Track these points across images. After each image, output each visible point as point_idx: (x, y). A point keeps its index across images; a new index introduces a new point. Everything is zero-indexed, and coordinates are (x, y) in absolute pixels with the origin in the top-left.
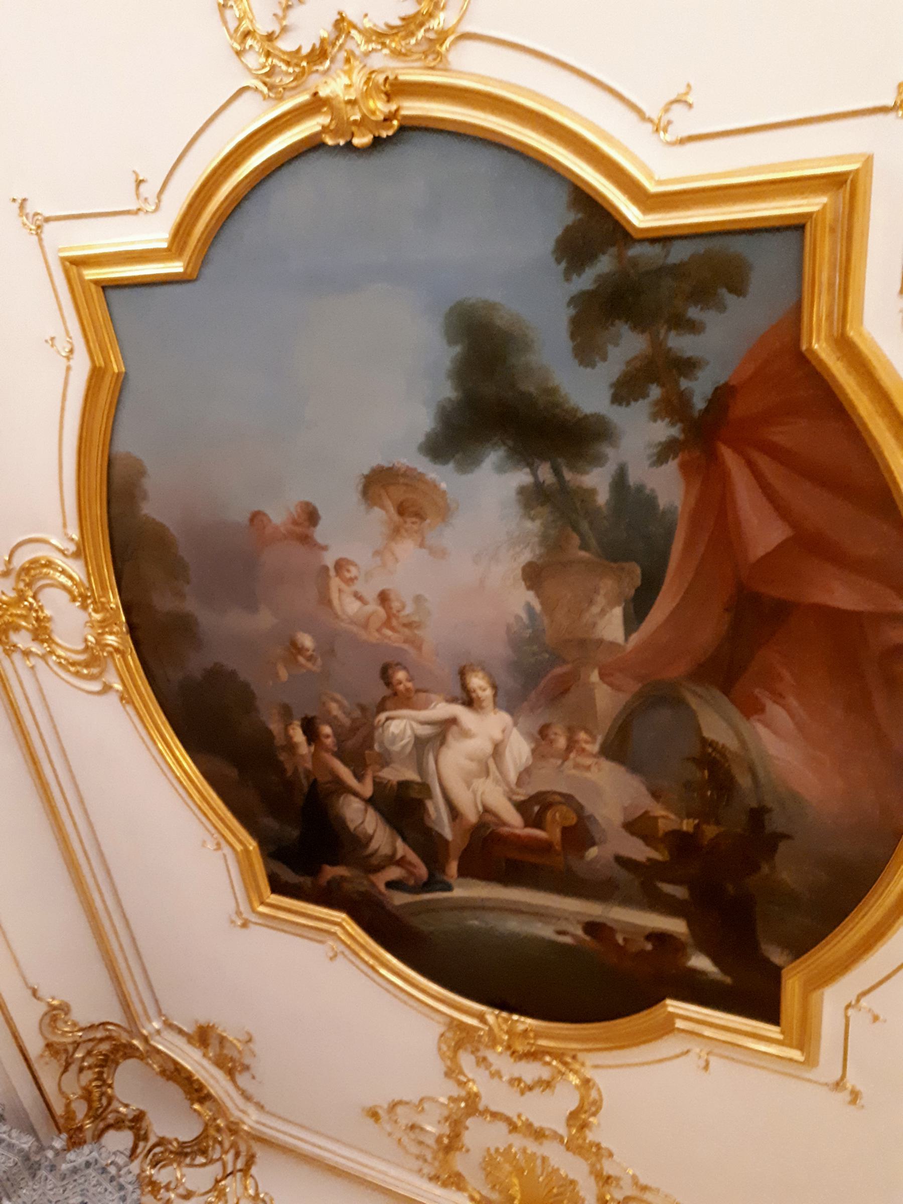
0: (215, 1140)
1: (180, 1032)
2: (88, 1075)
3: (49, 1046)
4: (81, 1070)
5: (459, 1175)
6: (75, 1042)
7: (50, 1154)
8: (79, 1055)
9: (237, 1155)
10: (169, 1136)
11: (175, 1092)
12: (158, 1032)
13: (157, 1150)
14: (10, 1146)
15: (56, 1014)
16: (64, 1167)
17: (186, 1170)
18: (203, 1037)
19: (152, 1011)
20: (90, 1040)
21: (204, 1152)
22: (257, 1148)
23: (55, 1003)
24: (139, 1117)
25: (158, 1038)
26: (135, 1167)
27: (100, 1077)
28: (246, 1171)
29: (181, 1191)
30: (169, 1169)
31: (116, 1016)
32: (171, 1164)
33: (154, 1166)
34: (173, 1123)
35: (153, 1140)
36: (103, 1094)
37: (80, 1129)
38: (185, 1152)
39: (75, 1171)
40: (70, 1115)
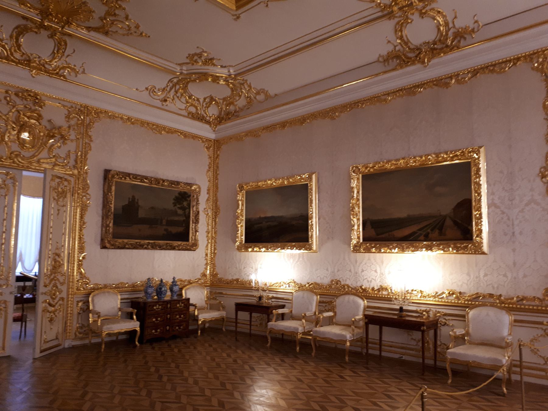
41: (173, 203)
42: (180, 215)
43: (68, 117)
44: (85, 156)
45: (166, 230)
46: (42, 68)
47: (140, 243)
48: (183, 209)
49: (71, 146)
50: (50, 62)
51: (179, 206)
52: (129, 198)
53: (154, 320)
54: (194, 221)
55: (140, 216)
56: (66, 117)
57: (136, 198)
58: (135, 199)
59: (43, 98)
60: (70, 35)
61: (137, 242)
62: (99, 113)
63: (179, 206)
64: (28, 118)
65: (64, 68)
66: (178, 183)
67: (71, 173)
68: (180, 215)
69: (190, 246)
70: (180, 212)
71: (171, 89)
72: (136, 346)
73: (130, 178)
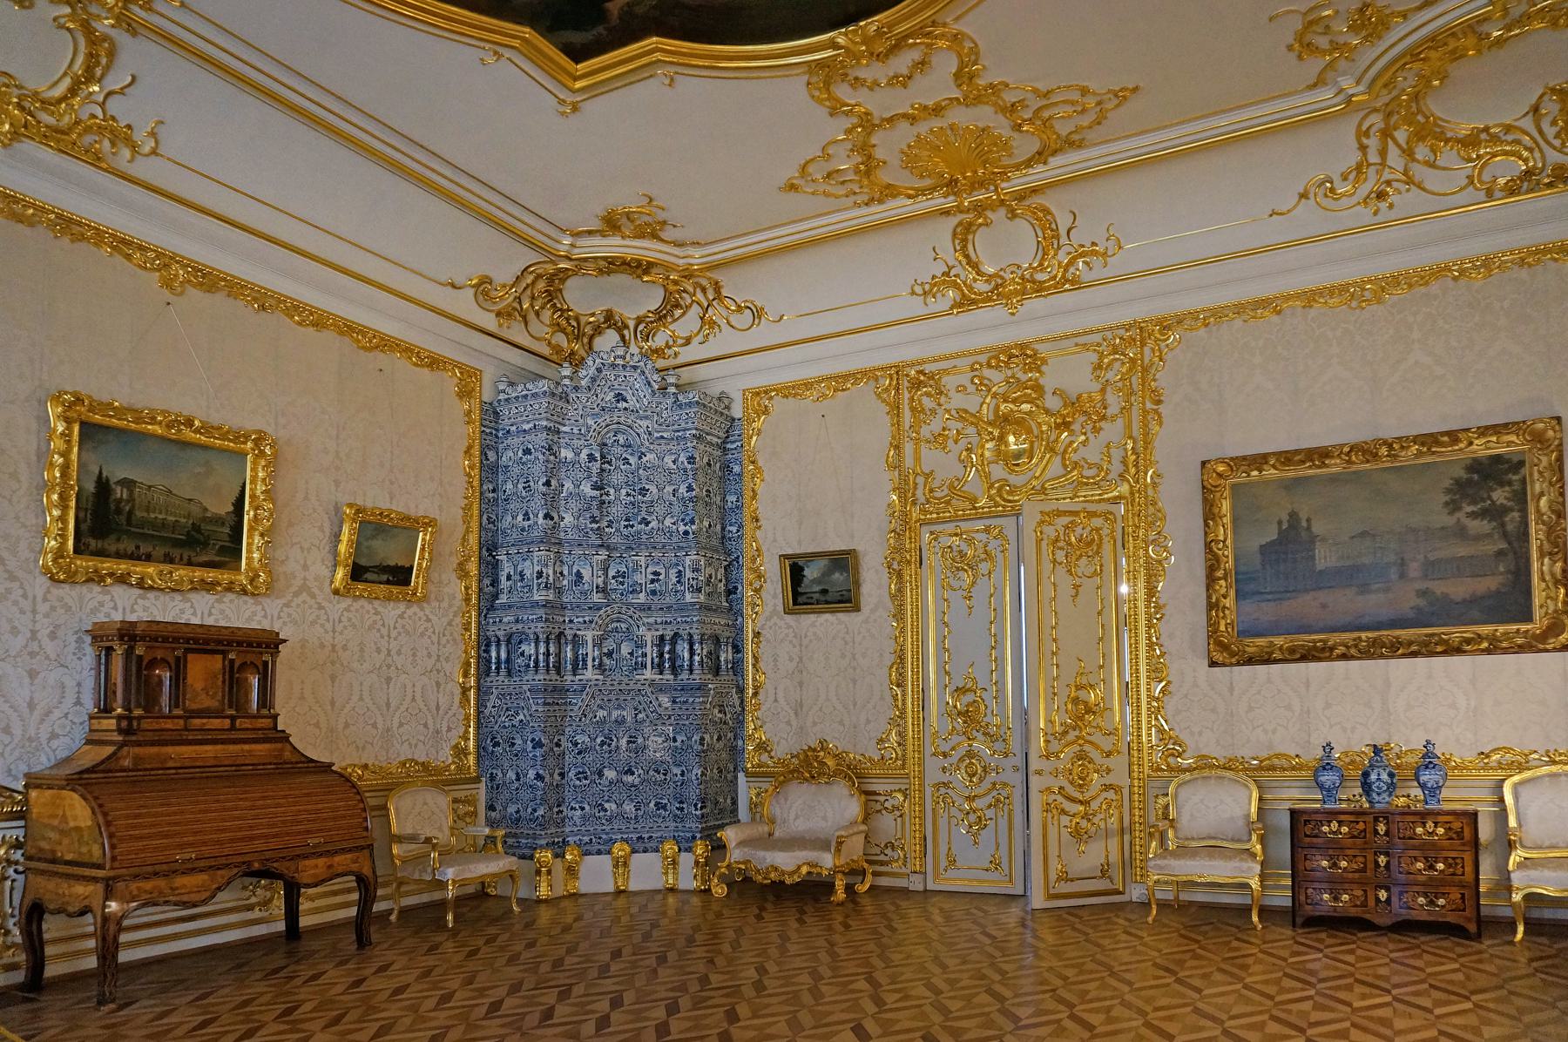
0: (679, 292)
1: (590, 233)
2: (547, 314)
3: (499, 314)
4: (537, 314)
5: (889, 186)
7: (567, 382)
9: (704, 290)
10: (642, 312)
12: (572, 245)
13: (641, 327)
15: (483, 288)
16: (583, 383)
18: (611, 224)
21: (677, 306)
22: (715, 275)
24: (609, 316)
26: (634, 349)
27: (555, 309)
29: (680, 341)
34: (641, 300)
35: (632, 324)
36: (568, 319)
37: (572, 353)
38: (661, 316)
39: (593, 380)
40: (558, 349)
41: (1447, 504)
42: (1477, 538)
46: (1033, 287)
48: (1495, 513)
50: (1041, 264)
51: (1469, 509)
52: (1280, 523)
54: (1547, 547)
55: (1321, 564)
56: (1095, 369)
57: (1303, 516)
58: (1298, 520)
63: (1469, 509)
64: (1014, 401)
65: (1071, 263)
66: (1453, 436)
67: (1116, 493)
68: (1477, 538)
69: (1535, 637)
70: (1476, 526)
71: (1383, 153)
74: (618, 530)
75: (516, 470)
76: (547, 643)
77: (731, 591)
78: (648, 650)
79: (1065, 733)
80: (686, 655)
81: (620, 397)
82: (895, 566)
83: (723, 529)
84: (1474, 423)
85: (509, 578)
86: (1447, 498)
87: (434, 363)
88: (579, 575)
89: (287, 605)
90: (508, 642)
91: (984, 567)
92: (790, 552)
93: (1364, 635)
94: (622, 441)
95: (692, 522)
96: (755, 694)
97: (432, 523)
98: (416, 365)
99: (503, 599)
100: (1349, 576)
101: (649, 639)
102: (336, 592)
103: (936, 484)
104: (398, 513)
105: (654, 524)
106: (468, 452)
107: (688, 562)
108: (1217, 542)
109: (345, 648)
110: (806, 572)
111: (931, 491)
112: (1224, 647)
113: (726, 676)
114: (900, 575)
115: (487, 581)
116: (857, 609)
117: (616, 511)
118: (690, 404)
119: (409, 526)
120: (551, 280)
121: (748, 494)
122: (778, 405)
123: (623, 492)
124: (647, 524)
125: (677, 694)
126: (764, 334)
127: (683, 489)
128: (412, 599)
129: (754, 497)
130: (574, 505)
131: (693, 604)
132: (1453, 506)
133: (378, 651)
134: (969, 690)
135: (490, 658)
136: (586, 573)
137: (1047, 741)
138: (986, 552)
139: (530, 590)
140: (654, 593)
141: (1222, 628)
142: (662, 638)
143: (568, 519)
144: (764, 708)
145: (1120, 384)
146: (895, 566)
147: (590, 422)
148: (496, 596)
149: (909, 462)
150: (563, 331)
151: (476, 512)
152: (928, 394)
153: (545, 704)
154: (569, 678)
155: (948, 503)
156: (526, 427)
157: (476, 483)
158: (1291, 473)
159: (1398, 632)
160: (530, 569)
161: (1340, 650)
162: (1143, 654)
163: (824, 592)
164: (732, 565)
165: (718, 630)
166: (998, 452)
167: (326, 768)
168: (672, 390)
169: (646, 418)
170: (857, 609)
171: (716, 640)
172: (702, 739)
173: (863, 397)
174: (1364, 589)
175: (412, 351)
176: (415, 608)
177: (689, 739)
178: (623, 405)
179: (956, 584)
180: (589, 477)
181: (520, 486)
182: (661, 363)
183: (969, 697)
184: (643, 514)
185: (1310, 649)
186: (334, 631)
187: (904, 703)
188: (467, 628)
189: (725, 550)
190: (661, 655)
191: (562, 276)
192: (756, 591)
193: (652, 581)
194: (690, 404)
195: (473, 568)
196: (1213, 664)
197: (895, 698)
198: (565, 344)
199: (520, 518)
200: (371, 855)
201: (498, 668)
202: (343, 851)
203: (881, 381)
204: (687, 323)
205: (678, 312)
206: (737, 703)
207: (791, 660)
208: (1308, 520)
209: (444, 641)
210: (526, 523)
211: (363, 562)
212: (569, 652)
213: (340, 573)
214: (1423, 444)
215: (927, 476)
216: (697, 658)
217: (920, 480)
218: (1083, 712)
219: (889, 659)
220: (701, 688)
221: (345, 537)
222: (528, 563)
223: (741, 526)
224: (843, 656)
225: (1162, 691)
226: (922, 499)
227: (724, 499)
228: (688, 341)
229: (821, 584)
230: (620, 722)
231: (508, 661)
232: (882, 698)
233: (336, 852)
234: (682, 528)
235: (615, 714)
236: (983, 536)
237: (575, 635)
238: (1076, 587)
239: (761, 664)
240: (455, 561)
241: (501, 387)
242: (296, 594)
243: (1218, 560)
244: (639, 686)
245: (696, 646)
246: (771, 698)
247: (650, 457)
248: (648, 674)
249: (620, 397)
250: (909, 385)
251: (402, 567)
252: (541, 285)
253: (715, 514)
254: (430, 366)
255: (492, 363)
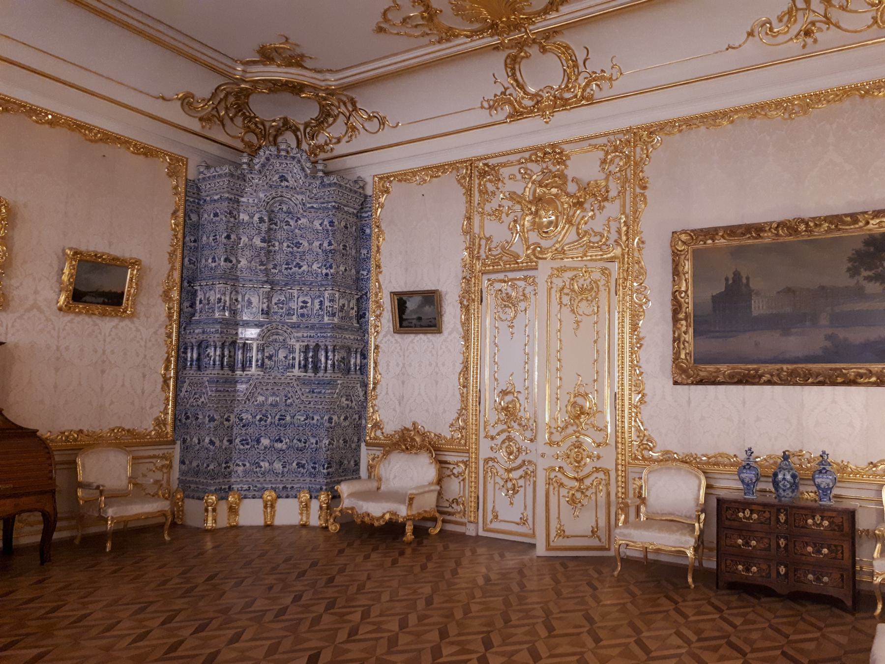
3: (201, 119)
6: (213, 109)
7: (245, 166)
8: (222, 113)
9: (345, 104)
10: (307, 119)
11: (287, 96)
13: (308, 130)
14: (220, 176)
17: (328, 130)
19: (229, 62)
20: (219, 103)
21: (329, 115)
22: (350, 94)
23: (181, 95)
25: (248, 75)
27: (245, 117)
28: (355, 109)
29: (334, 141)
30: (320, 135)
31: (222, 80)
32: (319, 132)
33: (313, 139)
34: (304, 113)
35: (302, 128)
39: (263, 165)
40: (249, 145)
41: (849, 270)
43: (604, 162)
44: (636, 220)
45: (829, 338)
47: (757, 370)
49: (612, 209)
52: (727, 279)
53: (740, 541)
55: (755, 313)
58: (740, 279)
59: (564, 146)
60: (556, 31)
61: (749, 370)
62: (652, 130)
72: (689, 587)
73: (723, 236)
74: (280, 271)
75: (209, 227)
76: (223, 347)
77: (361, 316)
78: (297, 355)
79: (567, 427)
80: (323, 360)
81: (283, 178)
82: (465, 303)
83: (358, 272)
84: (870, 208)
85: (201, 302)
86: (850, 265)
87: (148, 152)
88: (250, 303)
89: (21, 317)
90: (199, 346)
91: (522, 305)
92: (399, 290)
93: (785, 367)
94: (285, 209)
95: (331, 267)
96: (374, 388)
97: (136, 263)
98: (133, 153)
99: (196, 317)
100: (776, 322)
101: (297, 346)
102: (60, 309)
103: (493, 245)
104: (109, 255)
105: (305, 268)
106: (174, 214)
107: (326, 295)
108: (680, 293)
109: (67, 348)
110: (408, 304)
111: (490, 250)
112: (684, 371)
113: (352, 375)
114: (467, 309)
115: (186, 304)
116: (440, 331)
117: (280, 258)
118: (330, 185)
119: (119, 265)
120: (237, 96)
121: (374, 249)
122: (395, 187)
123: (285, 244)
124: (300, 267)
125: (314, 386)
126: (386, 136)
127: (326, 244)
128: (123, 315)
129: (378, 251)
130: (248, 253)
131: (328, 324)
132: (854, 272)
133: (95, 351)
134: (510, 392)
135: (186, 356)
136: (255, 300)
137: (551, 433)
138: (524, 295)
139: (213, 311)
140: (302, 315)
141: (683, 356)
142: (307, 347)
143: (244, 262)
144: (379, 398)
145: (618, 175)
146: (465, 303)
147: (262, 195)
148: (193, 315)
149: (476, 230)
150: (253, 132)
151: (179, 255)
152: (490, 181)
153: (217, 391)
154: (239, 373)
155: (500, 259)
156: (216, 197)
157: (180, 236)
158: (735, 242)
159: (810, 366)
160: (213, 296)
161: (767, 377)
162: (626, 373)
163: (420, 319)
164: (362, 300)
165: (348, 343)
166: (533, 223)
167: (33, 433)
168: (320, 174)
169: (302, 193)
170: (440, 331)
171: (349, 350)
172: (330, 419)
173: (449, 183)
174: (786, 332)
175: (130, 143)
176: (127, 322)
177: (322, 418)
178: (284, 184)
179: (504, 317)
180: (259, 233)
181: (211, 238)
182: (322, 156)
183: (509, 398)
184: (298, 260)
185: (745, 376)
186: (58, 337)
187: (467, 400)
188: (169, 336)
189: (358, 288)
190: (306, 359)
191: (247, 93)
192: (378, 317)
193: (302, 308)
194: (330, 185)
195: (175, 295)
196: (676, 383)
197: (462, 395)
198: (254, 140)
199: (210, 261)
200: (53, 497)
201: (191, 365)
202: (28, 494)
203: (461, 171)
204: (337, 129)
205: (331, 120)
206: (361, 394)
207: (398, 365)
208: (748, 279)
209: (149, 344)
210: (214, 265)
211: (83, 289)
212: (239, 355)
213: (62, 298)
214: (831, 223)
215: (488, 239)
216: (330, 362)
217: (483, 242)
218: (579, 413)
219: (459, 368)
220: (331, 383)
221: (66, 271)
222: (212, 292)
223: (369, 271)
224: (430, 364)
225: (640, 400)
226: (484, 256)
227: (358, 252)
228: (339, 140)
229: (418, 314)
230: (274, 405)
231: (198, 359)
232: (454, 395)
233: (22, 495)
234: (324, 271)
235: (271, 399)
236: (522, 284)
237: (245, 344)
238: (577, 322)
239: (379, 367)
240: (160, 290)
241: (202, 170)
242: (29, 310)
243: (680, 306)
244: (288, 381)
245: (330, 354)
246: (384, 393)
247: (303, 221)
248: (296, 372)
249: (283, 178)
250: (478, 174)
251: (115, 293)
252: (231, 99)
253: (350, 262)
254: (145, 155)
255: (195, 153)
